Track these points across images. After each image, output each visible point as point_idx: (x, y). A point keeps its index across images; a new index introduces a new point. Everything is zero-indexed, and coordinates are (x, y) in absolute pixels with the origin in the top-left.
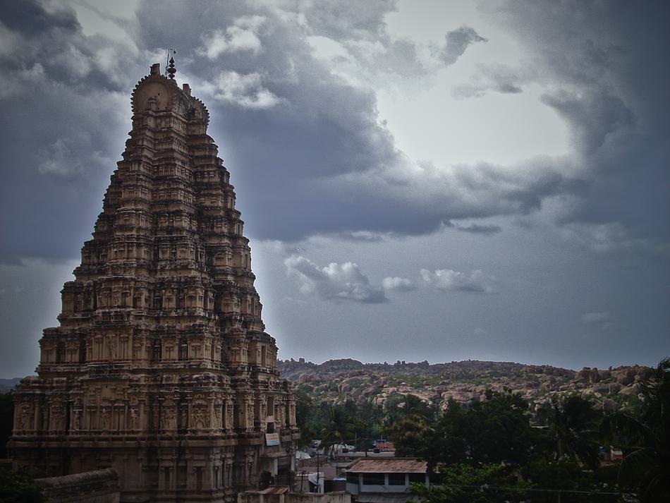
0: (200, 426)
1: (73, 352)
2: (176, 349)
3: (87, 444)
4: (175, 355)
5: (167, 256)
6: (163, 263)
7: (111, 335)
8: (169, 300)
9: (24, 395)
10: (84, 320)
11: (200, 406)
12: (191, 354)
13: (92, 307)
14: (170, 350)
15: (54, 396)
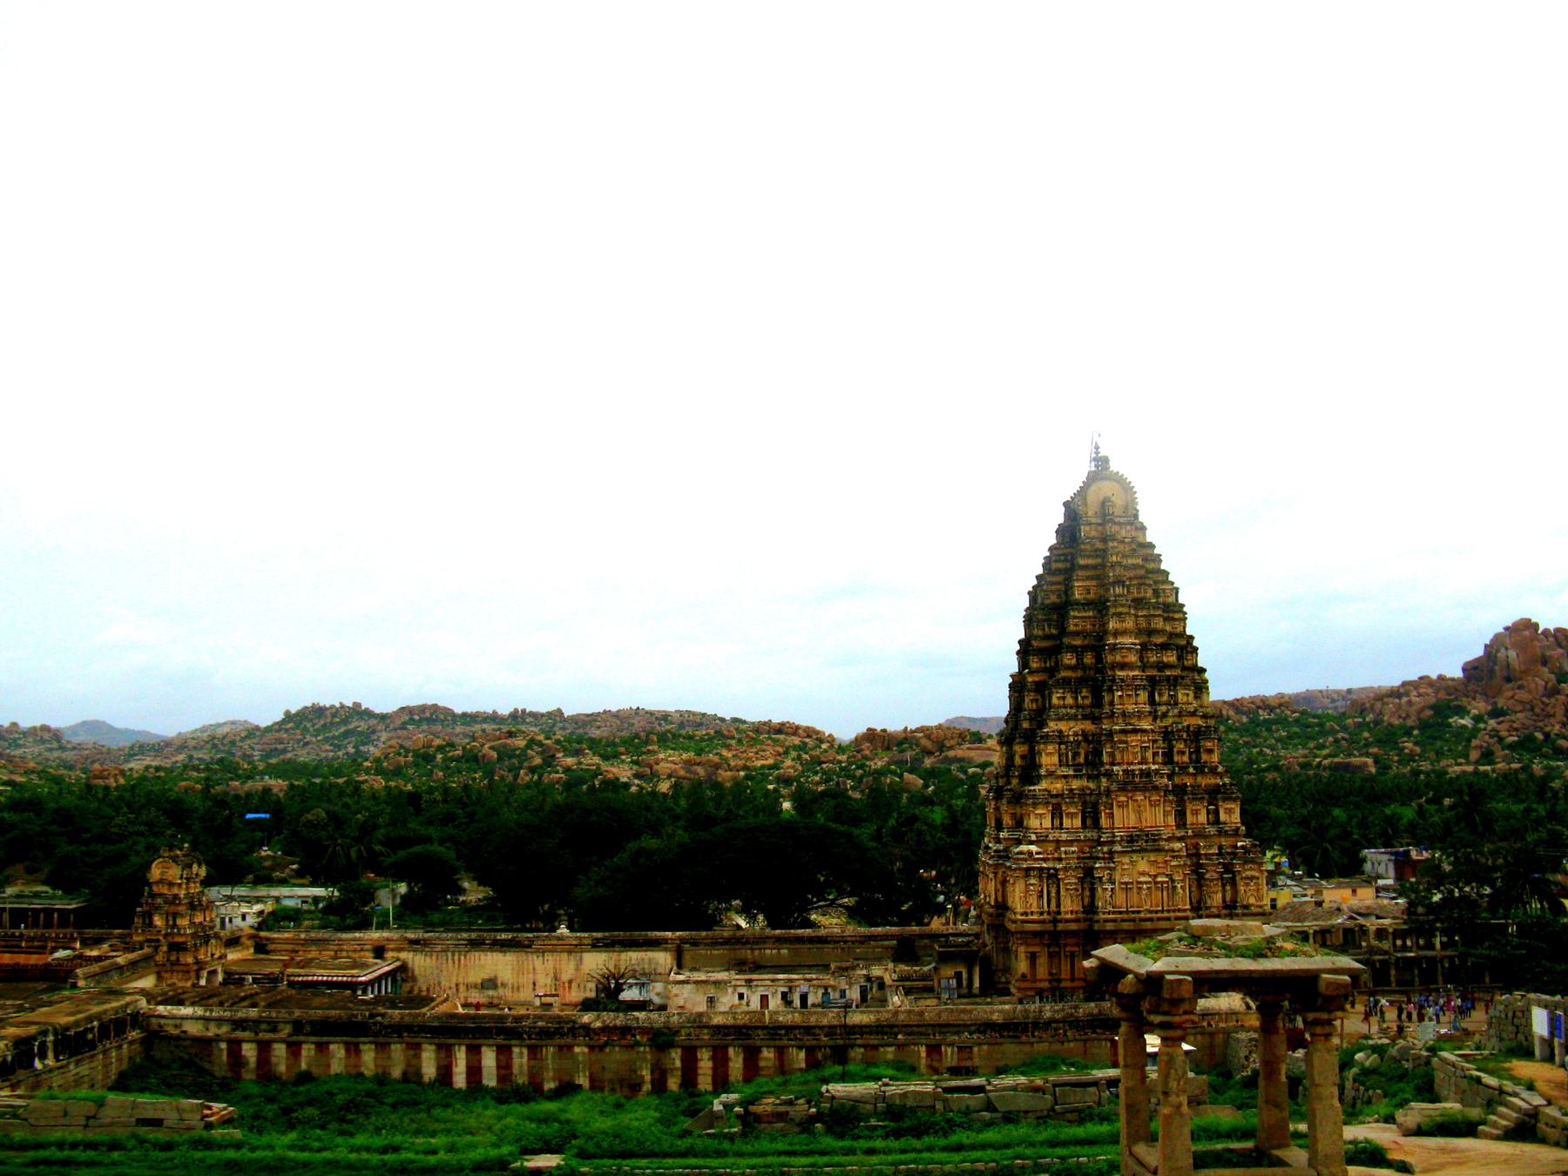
0: (1252, 901)
1: (1071, 816)
2: (1204, 812)
3: (1125, 926)
4: (1202, 818)
5: (1165, 698)
6: (1164, 708)
7: (1140, 798)
8: (1183, 753)
9: (1028, 869)
10: (1075, 777)
11: (1252, 878)
12: (1223, 817)
13: (1082, 760)
14: (1196, 813)
15: (1065, 869)
